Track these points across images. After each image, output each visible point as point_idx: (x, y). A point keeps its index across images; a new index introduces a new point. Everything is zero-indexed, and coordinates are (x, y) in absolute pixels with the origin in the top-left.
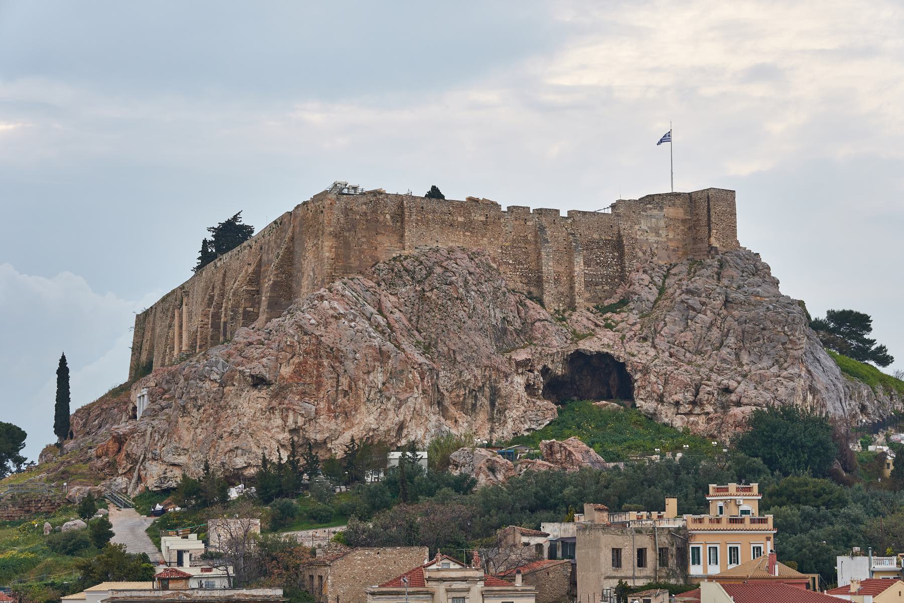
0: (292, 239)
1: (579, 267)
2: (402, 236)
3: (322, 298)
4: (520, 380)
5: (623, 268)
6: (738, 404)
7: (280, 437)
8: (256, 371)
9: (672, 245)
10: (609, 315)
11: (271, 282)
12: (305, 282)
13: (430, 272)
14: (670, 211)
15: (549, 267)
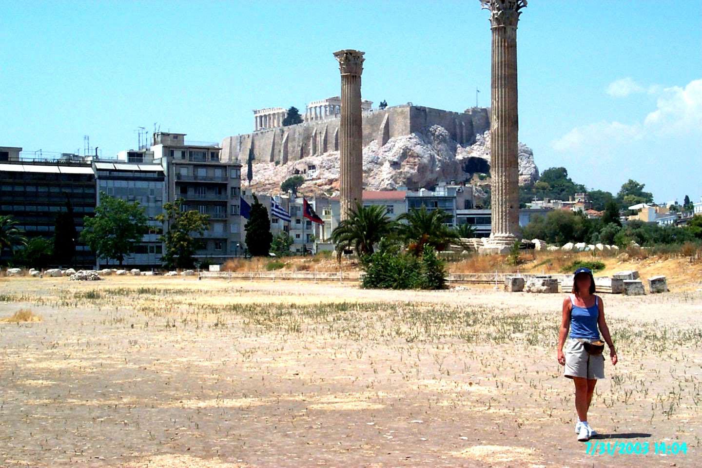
0: (388, 118)
1: (464, 131)
2: (426, 119)
3: (410, 138)
4: (460, 166)
5: (473, 132)
6: (522, 175)
7: (404, 180)
8: (396, 160)
9: (483, 124)
10: (473, 146)
11: (383, 132)
12: (396, 132)
13: (436, 132)
14: (482, 114)
15: (458, 131)
